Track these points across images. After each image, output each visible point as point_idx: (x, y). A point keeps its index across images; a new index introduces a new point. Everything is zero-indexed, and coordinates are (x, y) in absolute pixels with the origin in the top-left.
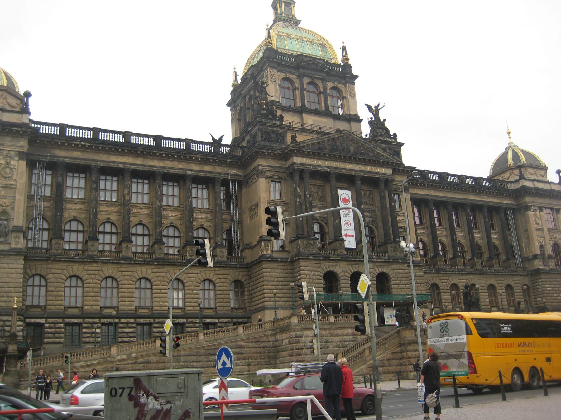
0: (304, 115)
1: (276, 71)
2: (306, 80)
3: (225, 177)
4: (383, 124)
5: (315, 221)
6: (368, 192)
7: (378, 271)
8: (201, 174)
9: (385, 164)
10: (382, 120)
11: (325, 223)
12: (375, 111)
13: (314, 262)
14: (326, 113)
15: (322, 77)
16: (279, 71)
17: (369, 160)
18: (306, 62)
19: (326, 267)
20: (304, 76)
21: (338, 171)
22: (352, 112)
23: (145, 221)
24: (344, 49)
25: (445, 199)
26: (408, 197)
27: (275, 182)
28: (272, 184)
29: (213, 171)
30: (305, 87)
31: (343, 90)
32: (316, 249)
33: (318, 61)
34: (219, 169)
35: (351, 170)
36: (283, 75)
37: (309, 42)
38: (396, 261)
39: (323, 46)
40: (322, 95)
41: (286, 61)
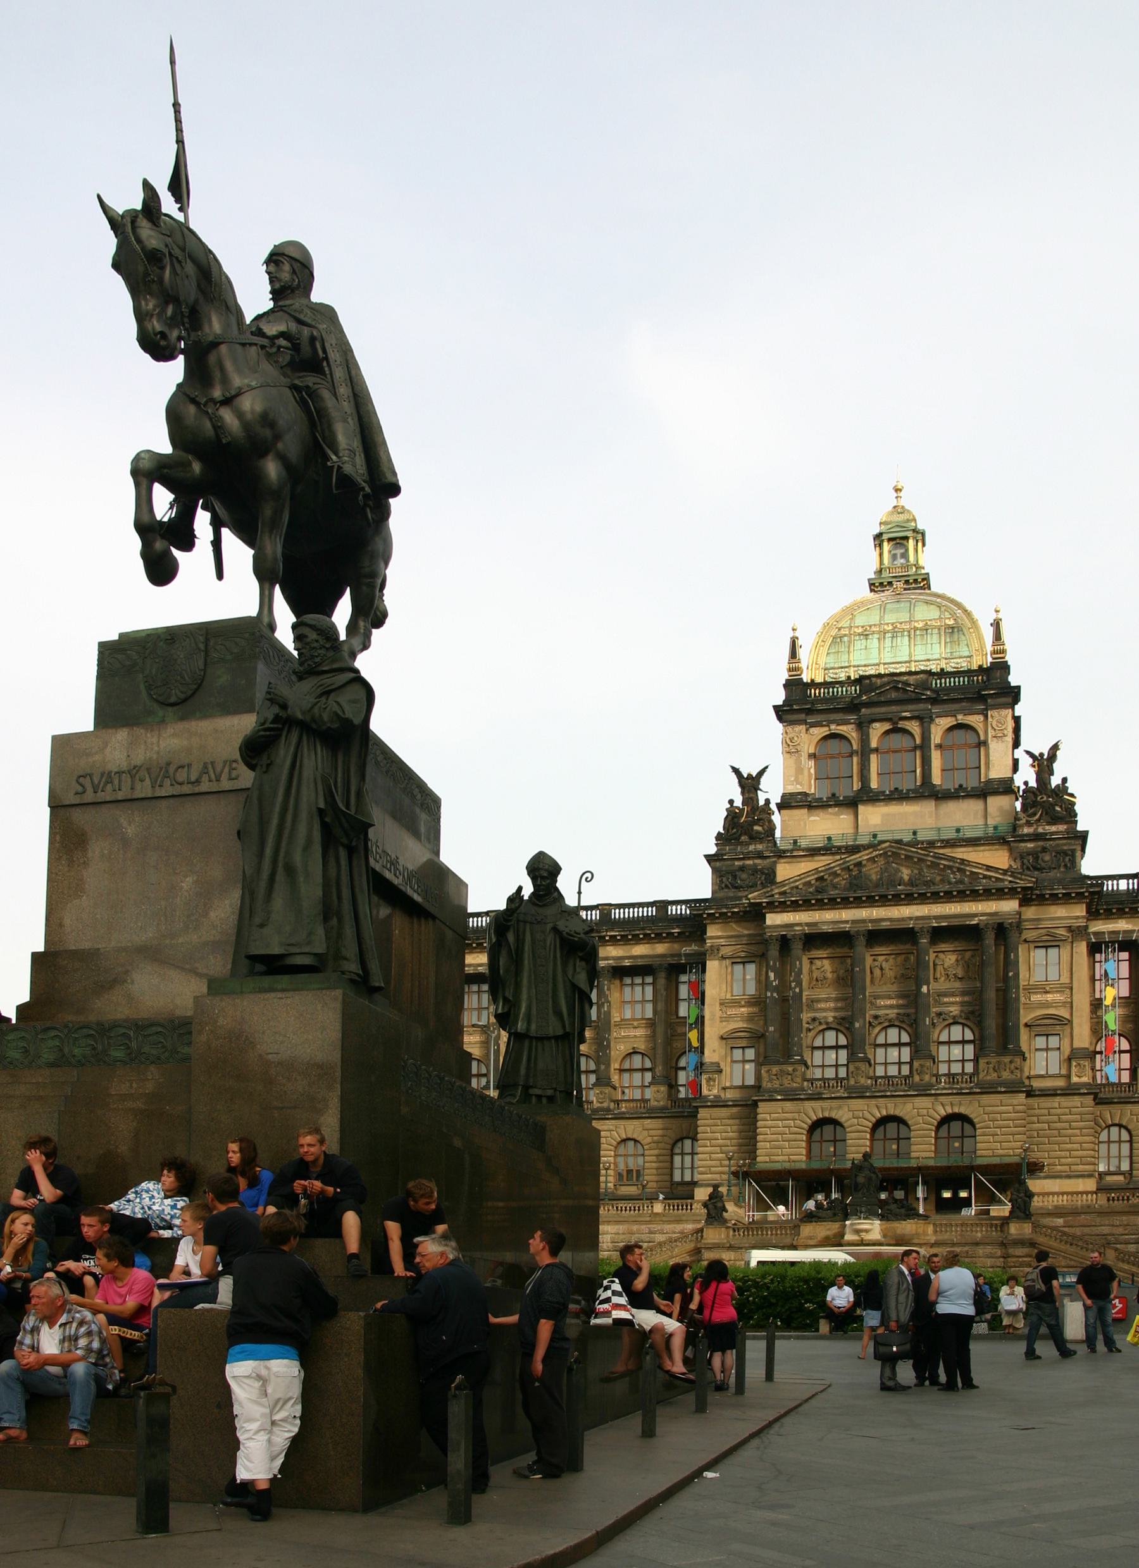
0: (861, 808)
1: (803, 727)
5: (824, 1027)
6: (968, 954)
11: (848, 1029)
13: (788, 1105)
14: (927, 792)
15: (916, 713)
16: (813, 725)
18: (877, 688)
19: (815, 1110)
22: (994, 774)
24: (997, 625)
27: (744, 963)
28: (738, 968)
30: (874, 744)
31: (980, 728)
32: (799, 1080)
33: (912, 679)
36: (819, 732)
37: (916, 629)
40: (918, 753)
41: (834, 698)
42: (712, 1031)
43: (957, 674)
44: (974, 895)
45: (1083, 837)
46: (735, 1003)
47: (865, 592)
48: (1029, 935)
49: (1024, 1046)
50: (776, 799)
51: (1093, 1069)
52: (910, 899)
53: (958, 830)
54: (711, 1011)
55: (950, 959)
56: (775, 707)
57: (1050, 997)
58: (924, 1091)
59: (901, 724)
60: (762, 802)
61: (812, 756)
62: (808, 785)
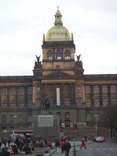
2: (56, 50)
3: (27, 85)
4: (81, 61)
7: (66, 112)
8: (20, 86)
9: (73, 79)
10: (80, 60)
12: (78, 58)
17: (66, 78)
20: (56, 48)
21: (56, 83)
22: (72, 58)
23: (6, 100)
24: (72, 34)
25: (107, 84)
26: (84, 87)
29: (24, 84)
30: (55, 52)
33: (60, 42)
34: (25, 84)
35: (60, 82)
36: (48, 50)
37: (61, 33)
38: (72, 108)
39: (66, 34)
42: (34, 98)
43: (66, 42)
44: (69, 79)
45: (84, 70)
46: (37, 94)
47: (53, 25)
48: (77, 84)
49: (76, 101)
50: (42, 60)
51: (86, 105)
52: (61, 79)
53: (67, 68)
54: (34, 95)
55: (66, 88)
56: (42, 46)
57: (79, 94)
58: (63, 108)
59: (59, 49)
60: (40, 61)
61: (47, 54)
62: (46, 58)
